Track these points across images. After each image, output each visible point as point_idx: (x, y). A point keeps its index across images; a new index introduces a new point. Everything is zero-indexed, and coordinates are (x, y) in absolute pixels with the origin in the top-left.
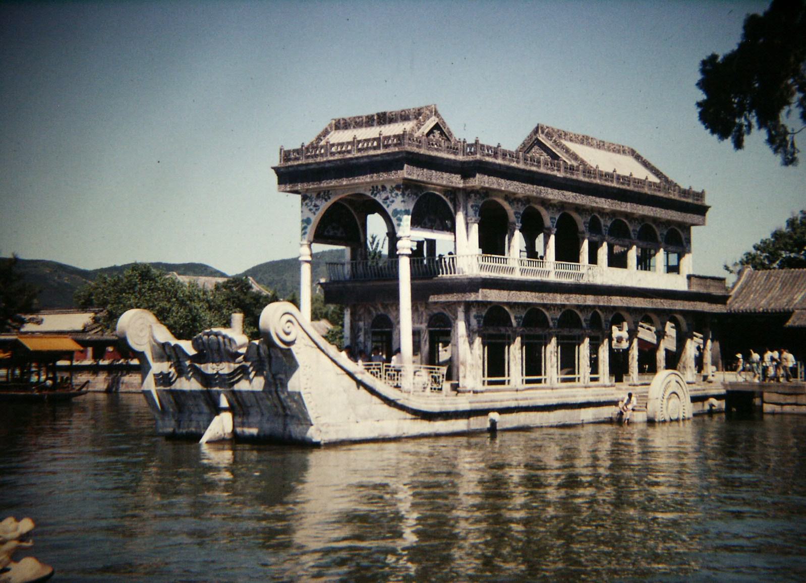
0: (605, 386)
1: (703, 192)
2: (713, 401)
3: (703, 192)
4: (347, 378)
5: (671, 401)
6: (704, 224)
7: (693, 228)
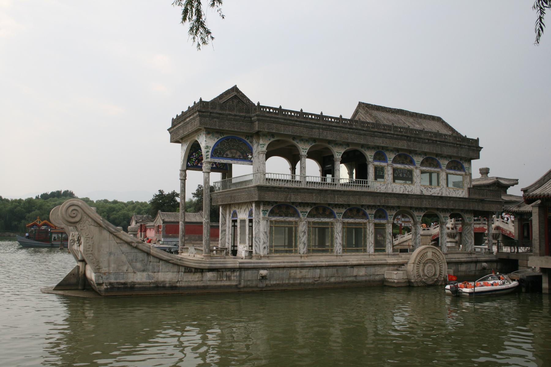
0: (388, 255)
1: (478, 139)
2: (484, 264)
3: (478, 139)
4: (126, 246)
5: (428, 265)
6: (478, 157)
7: (472, 161)
